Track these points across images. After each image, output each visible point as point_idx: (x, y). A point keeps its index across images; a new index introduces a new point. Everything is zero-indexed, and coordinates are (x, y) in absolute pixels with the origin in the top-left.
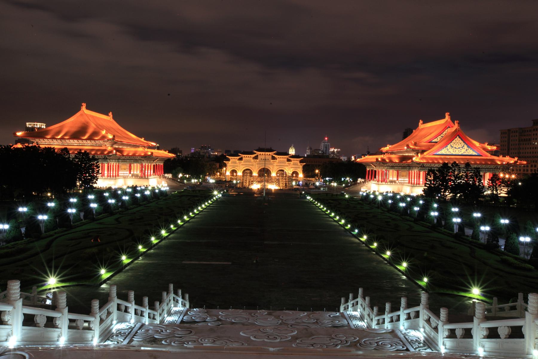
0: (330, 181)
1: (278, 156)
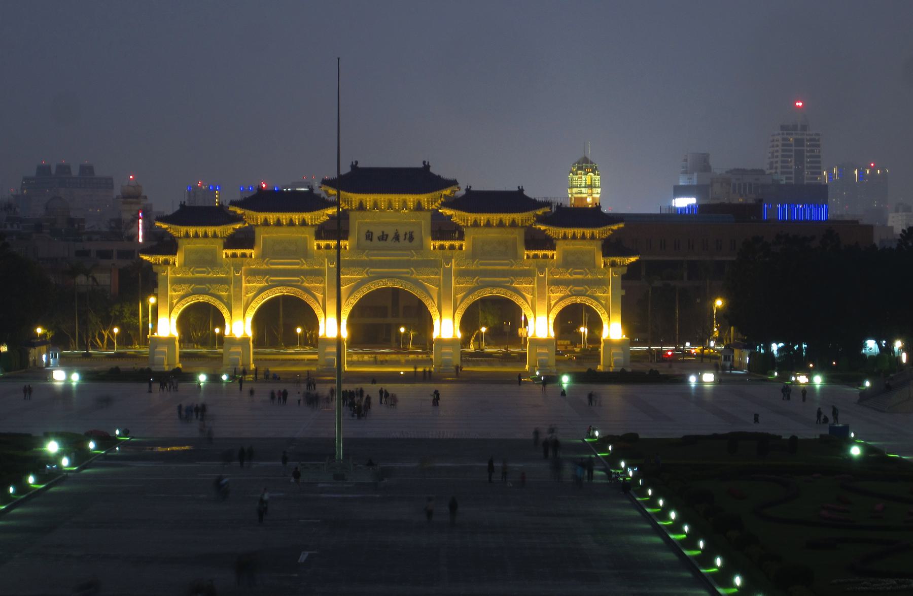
0: (792, 362)
1: (471, 217)
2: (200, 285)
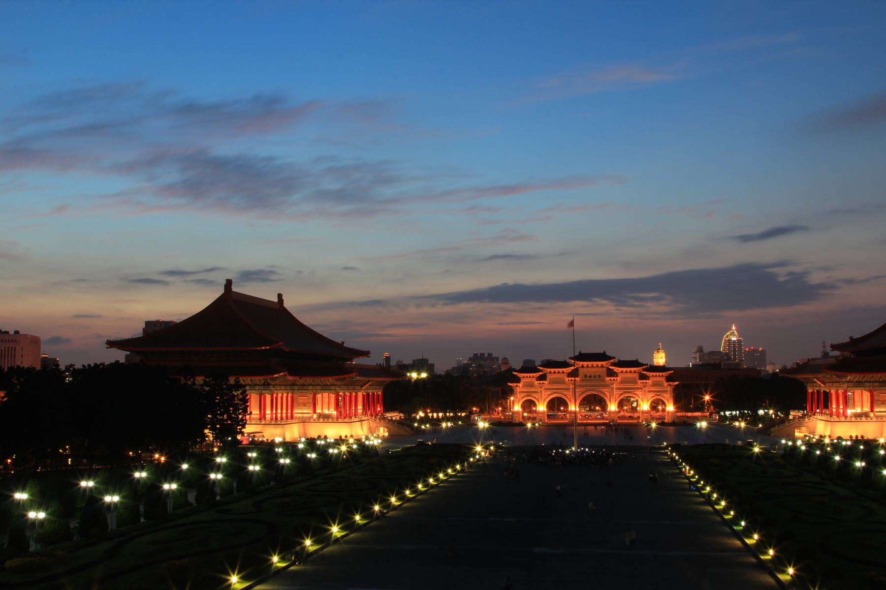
1: (620, 369)
2: (529, 393)
